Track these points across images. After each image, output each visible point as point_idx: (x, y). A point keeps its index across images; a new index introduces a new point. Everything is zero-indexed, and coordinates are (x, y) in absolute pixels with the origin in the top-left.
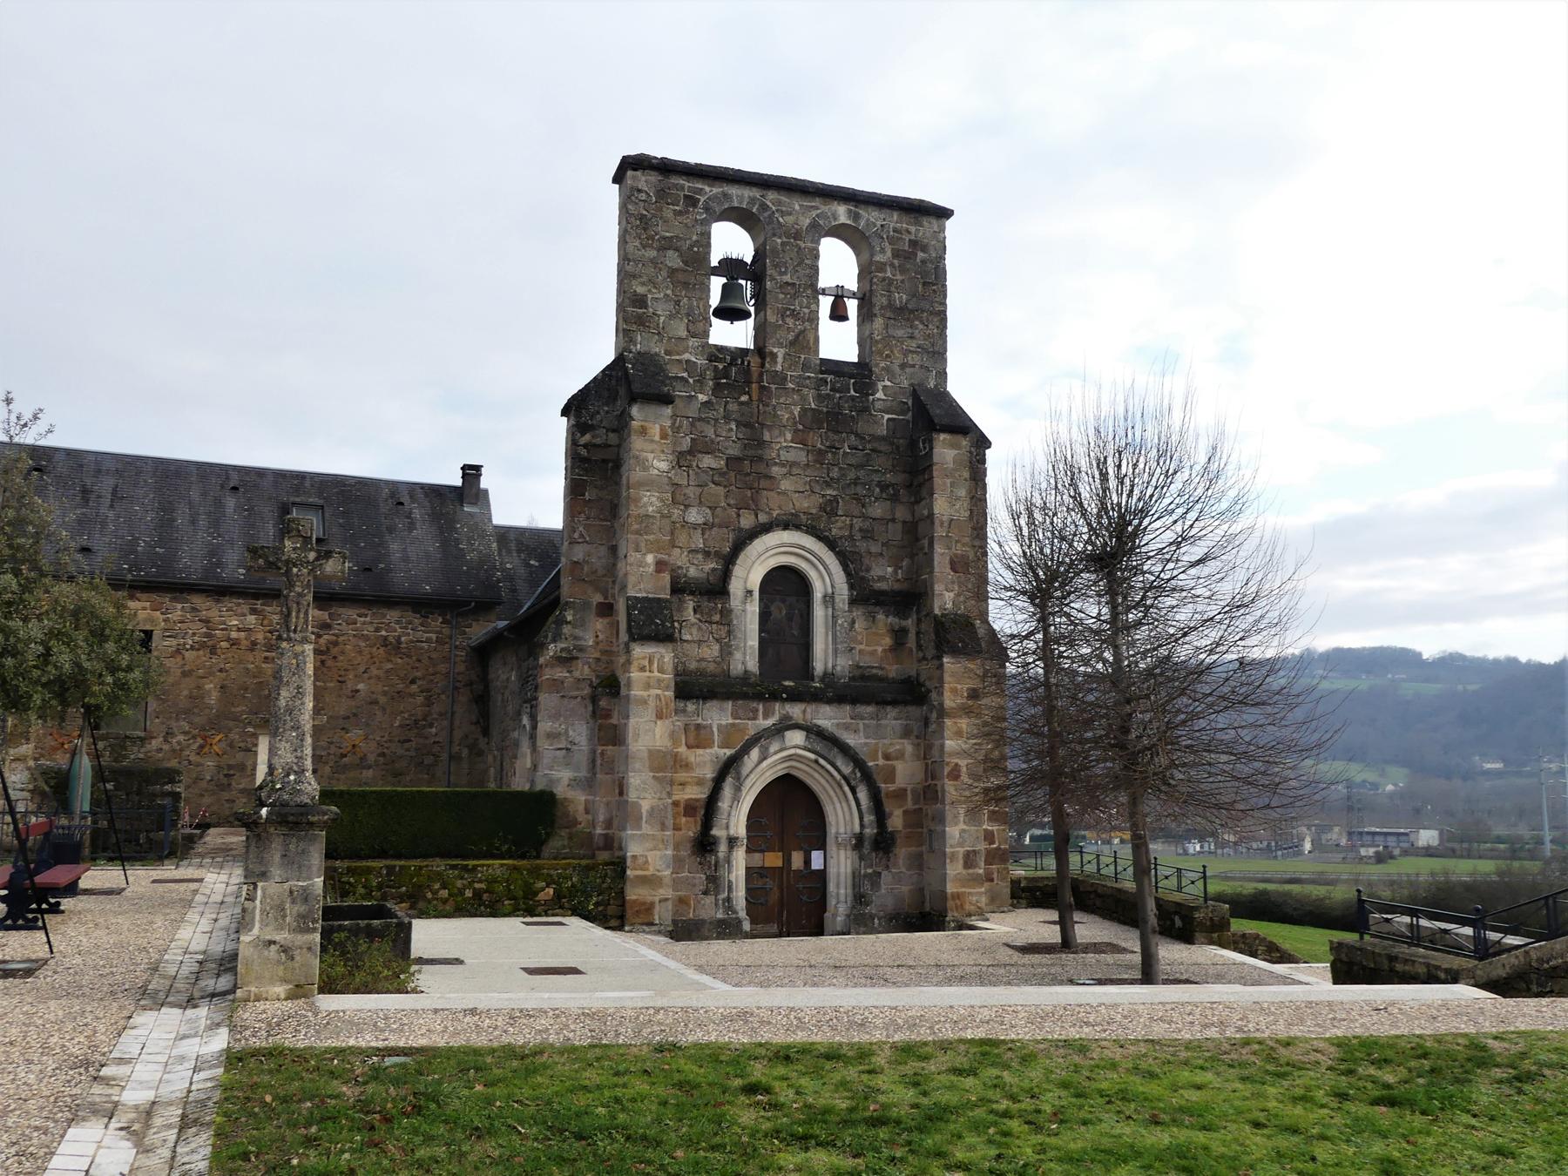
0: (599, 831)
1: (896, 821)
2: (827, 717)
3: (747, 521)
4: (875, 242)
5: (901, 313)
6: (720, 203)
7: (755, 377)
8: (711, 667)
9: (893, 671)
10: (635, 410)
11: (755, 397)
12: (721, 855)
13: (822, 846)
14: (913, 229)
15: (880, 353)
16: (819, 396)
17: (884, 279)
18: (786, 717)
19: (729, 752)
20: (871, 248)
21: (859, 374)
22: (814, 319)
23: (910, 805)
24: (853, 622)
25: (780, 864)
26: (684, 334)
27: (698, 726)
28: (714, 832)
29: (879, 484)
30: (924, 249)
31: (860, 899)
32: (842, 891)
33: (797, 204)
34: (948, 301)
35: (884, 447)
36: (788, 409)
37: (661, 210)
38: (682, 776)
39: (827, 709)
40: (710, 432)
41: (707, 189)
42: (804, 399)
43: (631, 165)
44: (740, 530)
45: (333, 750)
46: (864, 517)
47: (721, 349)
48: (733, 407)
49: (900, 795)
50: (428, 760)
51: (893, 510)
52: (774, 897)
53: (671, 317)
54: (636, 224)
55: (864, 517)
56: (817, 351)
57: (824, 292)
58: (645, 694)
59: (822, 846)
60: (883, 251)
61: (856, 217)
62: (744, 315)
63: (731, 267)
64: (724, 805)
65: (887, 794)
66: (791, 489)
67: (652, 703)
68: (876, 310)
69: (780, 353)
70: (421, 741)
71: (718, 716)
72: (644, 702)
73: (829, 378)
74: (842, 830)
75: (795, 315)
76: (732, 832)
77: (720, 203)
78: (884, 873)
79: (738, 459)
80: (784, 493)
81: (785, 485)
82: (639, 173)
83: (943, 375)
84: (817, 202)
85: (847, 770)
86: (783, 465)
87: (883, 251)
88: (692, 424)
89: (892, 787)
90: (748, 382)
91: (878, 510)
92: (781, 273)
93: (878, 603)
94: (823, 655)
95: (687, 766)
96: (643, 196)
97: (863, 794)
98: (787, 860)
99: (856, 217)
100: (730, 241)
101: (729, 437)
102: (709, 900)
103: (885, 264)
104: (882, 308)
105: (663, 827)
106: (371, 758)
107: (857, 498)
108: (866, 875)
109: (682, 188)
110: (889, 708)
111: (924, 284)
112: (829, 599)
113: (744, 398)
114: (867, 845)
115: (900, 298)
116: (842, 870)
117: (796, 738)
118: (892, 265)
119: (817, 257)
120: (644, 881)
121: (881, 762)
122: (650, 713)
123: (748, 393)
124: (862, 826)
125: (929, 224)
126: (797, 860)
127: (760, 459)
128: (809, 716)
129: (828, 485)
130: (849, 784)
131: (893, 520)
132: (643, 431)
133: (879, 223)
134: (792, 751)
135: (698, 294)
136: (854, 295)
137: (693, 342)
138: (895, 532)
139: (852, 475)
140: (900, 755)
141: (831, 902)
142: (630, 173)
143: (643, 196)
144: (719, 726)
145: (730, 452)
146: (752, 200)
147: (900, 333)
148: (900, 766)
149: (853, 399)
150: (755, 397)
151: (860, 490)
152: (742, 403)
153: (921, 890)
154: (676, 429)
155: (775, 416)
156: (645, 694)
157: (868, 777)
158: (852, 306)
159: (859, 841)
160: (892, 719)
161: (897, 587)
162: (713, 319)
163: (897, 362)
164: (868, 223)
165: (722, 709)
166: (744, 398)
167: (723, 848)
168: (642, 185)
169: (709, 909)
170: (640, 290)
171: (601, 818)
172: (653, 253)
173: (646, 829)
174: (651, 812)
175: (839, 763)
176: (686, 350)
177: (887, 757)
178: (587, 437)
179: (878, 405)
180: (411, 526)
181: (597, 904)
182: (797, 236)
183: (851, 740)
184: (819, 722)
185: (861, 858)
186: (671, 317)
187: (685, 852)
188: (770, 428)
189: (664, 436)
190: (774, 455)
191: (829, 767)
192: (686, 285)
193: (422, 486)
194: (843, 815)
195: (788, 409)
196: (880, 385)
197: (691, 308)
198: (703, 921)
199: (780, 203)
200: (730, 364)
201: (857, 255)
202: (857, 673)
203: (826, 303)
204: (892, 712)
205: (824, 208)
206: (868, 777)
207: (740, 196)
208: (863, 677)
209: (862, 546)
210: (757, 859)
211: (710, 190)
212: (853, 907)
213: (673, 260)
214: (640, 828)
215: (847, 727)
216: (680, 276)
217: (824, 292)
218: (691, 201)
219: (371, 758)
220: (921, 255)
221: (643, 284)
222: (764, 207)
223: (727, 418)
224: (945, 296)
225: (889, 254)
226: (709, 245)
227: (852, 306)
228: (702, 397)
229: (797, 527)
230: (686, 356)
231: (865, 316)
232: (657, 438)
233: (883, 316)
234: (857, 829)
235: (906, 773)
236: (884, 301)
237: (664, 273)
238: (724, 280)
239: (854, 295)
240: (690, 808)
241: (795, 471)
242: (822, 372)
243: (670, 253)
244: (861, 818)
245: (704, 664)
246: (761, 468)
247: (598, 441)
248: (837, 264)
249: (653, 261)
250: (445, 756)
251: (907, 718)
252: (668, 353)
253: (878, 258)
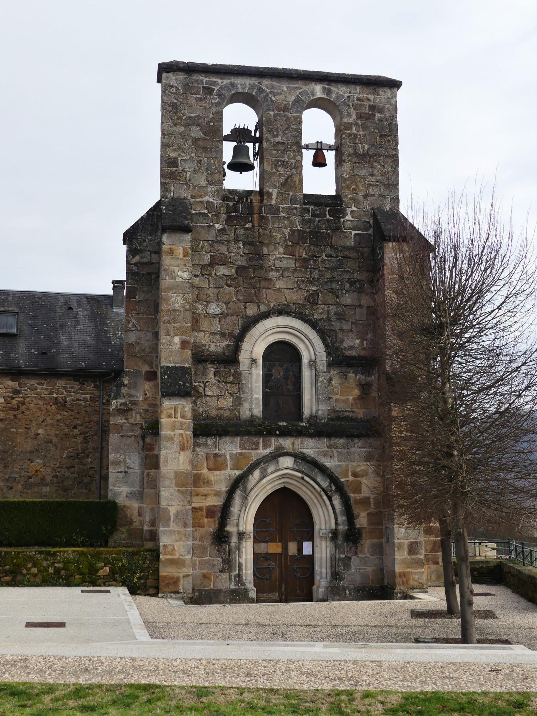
0: (146, 528)
1: (362, 520)
2: (310, 447)
3: (252, 311)
4: (344, 109)
5: (364, 158)
6: (229, 90)
7: (256, 210)
8: (227, 414)
9: (360, 413)
10: (165, 238)
11: (256, 224)
12: (233, 544)
13: (311, 539)
14: (372, 97)
15: (348, 187)
16: (303, 220)
17: (350, 135)
18: (280, 448)
19: (238, 473)
20: (341, 113)
21: (334, 204)
22: (299, 167)
23: (372, 510)
24: (331, 379)
25: (280, 551)
26: (203, 182)
27: (216, 455)
28: (228, 528)
29: (349, 281)
30: (381, 111)
31: (335, 576)
32: (324, 570)
33: (285, 86)
34: (399, 147)
35: (352, 254)
36: (280, 231)
37: (186, 98)
38: (204, 489)
39: (310, 442)
40: (224, 250)
41: (219, 81)
42: (292, 223)
43: (165, 69)
44: (247, 317)
45: (23, 473)
46: (338, 304)
47: (232, 192)
48: (240, 232)
49: (365, 502)
50: (86, 480)
51: (359, 299)
52: (276, 574)
53: (195, 172)
54: (170, 110)
55: (338, 304)
56: (301, 189)
57: (307, 147)
58: (172, 433)
59: (311, 539)
60: (349, 115)
61: (329, 92)
62: (250, 167)
63: (240, 135)
65: (356, 501)
66: (284, 287)
67: (177, 440)
68: (345, 157)
69: (274, 192)
70: (81, 467)
71: (230, 447)
72: (171, 439)
73: (311, 207)
74: (323, 527)
75: (284, 164)
76: (241, 529)
77: (229, 90)
78: (354, 558)
79: (244, 268)
80: (279, 290)
81: (279, 284)
82: (171, 74)
83: (396, 200)
84: (300, 84)
85: (325, 484)
86: (277, 271)
87: (349, 115)
88: (211, 246)
89: (358, 497)
90: (251, 214)
91: (348, 299)
92: (274, 136)
93: (349, 365)
94: (310, 403)
95: (208, 483)
96: (174, 90)
97: (337, 501)
98: (285, 548)
99: (329, 92)
100: (239, 116)
101: (238, 253)
102: (225, 576)
103: (351, 124)
104: (349, 155)
105: (185, 525)
106: (48, 478)
107: (332, 291)
108: (340, 559)
109: (202, 82)
110: (356, 440)
111: (381, 136)
112: (313, 364)
113: (249, 225)
115: (362, 147)
116: (324, 555)
117: (287, 462)
118: (356, 124)
119: (300, 123)
120: (174, 562)
121: (351, 478)
122: (175, 447)
123: (251, 221)
124: (337, 524)
125: (384, 93)
126: (292, 548)
127: (261, 267)
129: (310, 283)
130: (327, 495)
131: (360, 306)
132: (171, 252)
133: (346, 95)
134: (285, 472)
135: (214, 155)
136: (330, 148)
137: (211, 188)
138: (360, 314)
139: (328, 275)
140: (365, 474)
141: (317, 578)
142: (164, 75)
143: (174, 90)
144: (231, 455)
145: (239, 263)
146: (252, 87)
147: (363, 172)
148: (364, 480)
149: (328, 221)
150: (256, 224)
151: (334, 286)
152: (247, 229)
153: (382, 570)
154: (195, 250)
155: (271, 236)
156: (172, 433)
157: (340, 489)
158: (330, 156)
159: (334, 535)
160: (358, 448)
161: (363, 353)
162: (228, 171)
163: (361, 193)
164: (338, 96)
165: (232, 442)
166: (249, 225)
167: (234, 540)
168: (173, 82)
169: (225, 582)
170: (173, 155)
171: (147, 519)
172: (182, 129)
173: (173, 526)
174: (177, 515)
175: (319, 479)
176: (206, 194)
177: (355, 475)
178: (137, 258)
179: (347, 225)
180: (77, 323)
181: (139, 578)
182: (286, 109)
183: (328, 463)
184: (304, 451)
185: (336, 547)
186: (195, 172)
187: (207, 543)
188: (267, 245)
189: (186, 254)
190: (271, 264)
191: (312, 482)
192: (205, 149)
193: (86, 296)
194: (325, 516)
195: (280, 231)
196: (348, 211)
197: (209, 164)
198: (220, 591)
199: (272, 87)
200: (238, 202)
201: (334, 119)
202: (333, 415)
203: (308, 156)
204: (358, 442)
205: (305, 88)
206: (340, 489)
207: (243, 84)
208: (339, 418)
209: (337, 325)
210: (263, 548)
211: (221, 82)
212: (331, 582)
213: (196, 132)
214: (168, 526)
215: (325, 454)
216: (201, 143)
217: (307, 147)
218: (208, 91)
219: (48, 478)
220: (378, 115)
221: (175, 150)
222: (261, 90)
223: (236, 239)
224: (397, 144)
225: (354, 116)
226: (221, 120)
227: (330, 156)
228: (218, 226)
229: (288, 314)
230: (207, 198)
231: (339, 162)
232: (181, 256)
233: (350, 161)
234: (333, 526)
235: (368, 486)
236: (351, 150)
237: (190, 142)
238: (235, 144)
239: (330, 148)
240: (210, 512)
241: (286, 274)
242: (305, 204)
243: (194, 128)
244: (336, 519)
245: (222, 412)
246: (262, 273)
247: (145, 260)
248: (318, 127)
249: (182, 135)
250: (97, 477)
251: (370, 447)
252: (193, 197)
253: (347, 120)
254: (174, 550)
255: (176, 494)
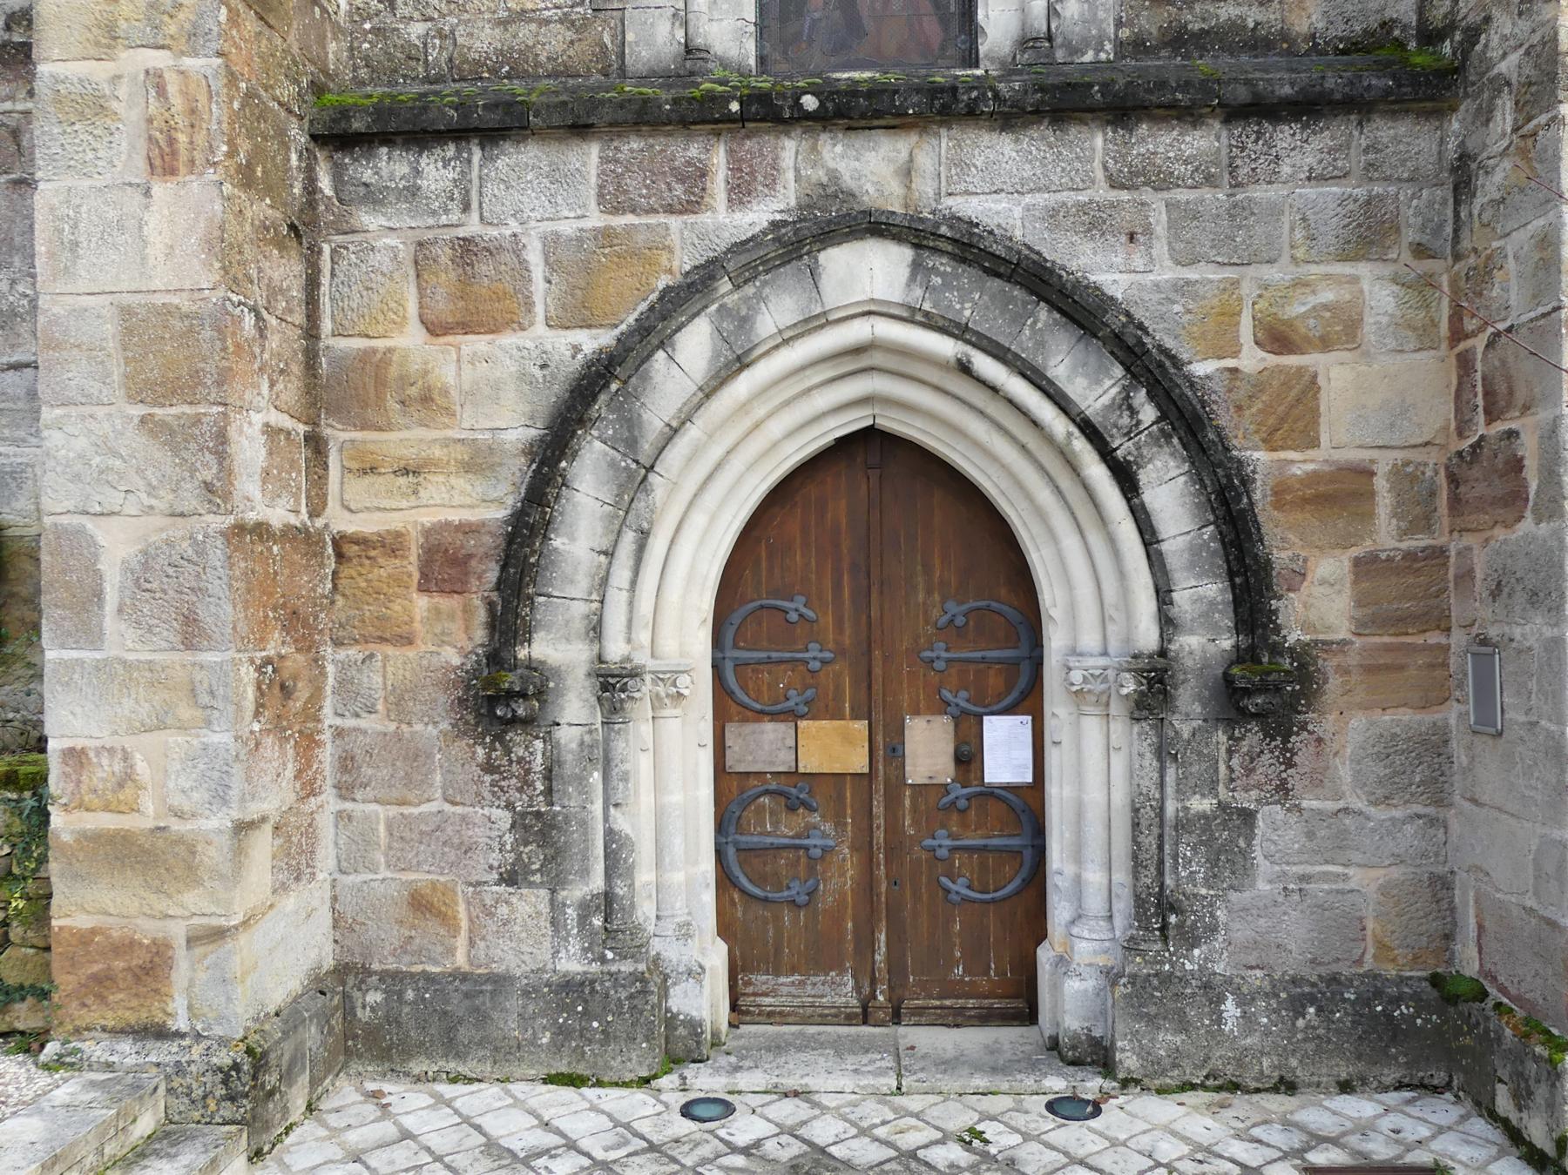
1: (1320, 601)
2: (1003, 183)
8: (554, 43)
12: (567, 736)
13: (1026, 696)
19: (593, 341)
25: (858, 761)
27: (467, 249)
28: (541, 648)
31: (1160, 913)
32: (1094, 877)
38: (404, 439)
49: (1342, 493)
52: (843, 876)
58: (99, 71)
59: (1026, 696)
64: (579, 532)
65: (1281, 494)
67: (130, 110)
71: (542, 199)
72: (92, 106)
74: (1090, 640)
76: (615, 649)
78: (1269, 816)
85: (1097, 388)
89: (1302, 463)
95: (428, 401)
97: (1168, 488)
102: (530, 903)
105: (191, 633)
108: (1181, 825)
110: (1285, 136)
114: (1189, 709)
116: (1094, 795)
120: (144, 856)
122: (125, 153)
124: (1167, 622)
126: (927, 750)
128: (925, 187)
130: (1106, 454)
134: (858, 331)
140: (1343, 330)
141: (1059, 912)
144: (552, 244)
148: (1336, 375)
153: (1441, 885)
156: (99, 71)
157: (1188, 422)
159: (1155, 684)
160: (1301, 175)
165: (556, 176)
167: (575, 710)
169: (528, 939)
173: (120, 638)
174: (141, 575)
175: (1060, 368)
177: (1278, 338)
183: (1109, 271)
184: (970, 207)
185: (1164, 752)
187: (432, 728)
191: (1018, 388)
198: (500, 982)
204: (1297, 149)
206: (1188, 422)
210: (766, 746)
212: (1131, 947)
214: (93, 637)
215: (1094, 222)
234: (1147, 636)
235: (1371, 399)
240: (443, 563)
244: (1163, 594)
245: (525, 32)
254: (127, 779)
255: (135, 442)
